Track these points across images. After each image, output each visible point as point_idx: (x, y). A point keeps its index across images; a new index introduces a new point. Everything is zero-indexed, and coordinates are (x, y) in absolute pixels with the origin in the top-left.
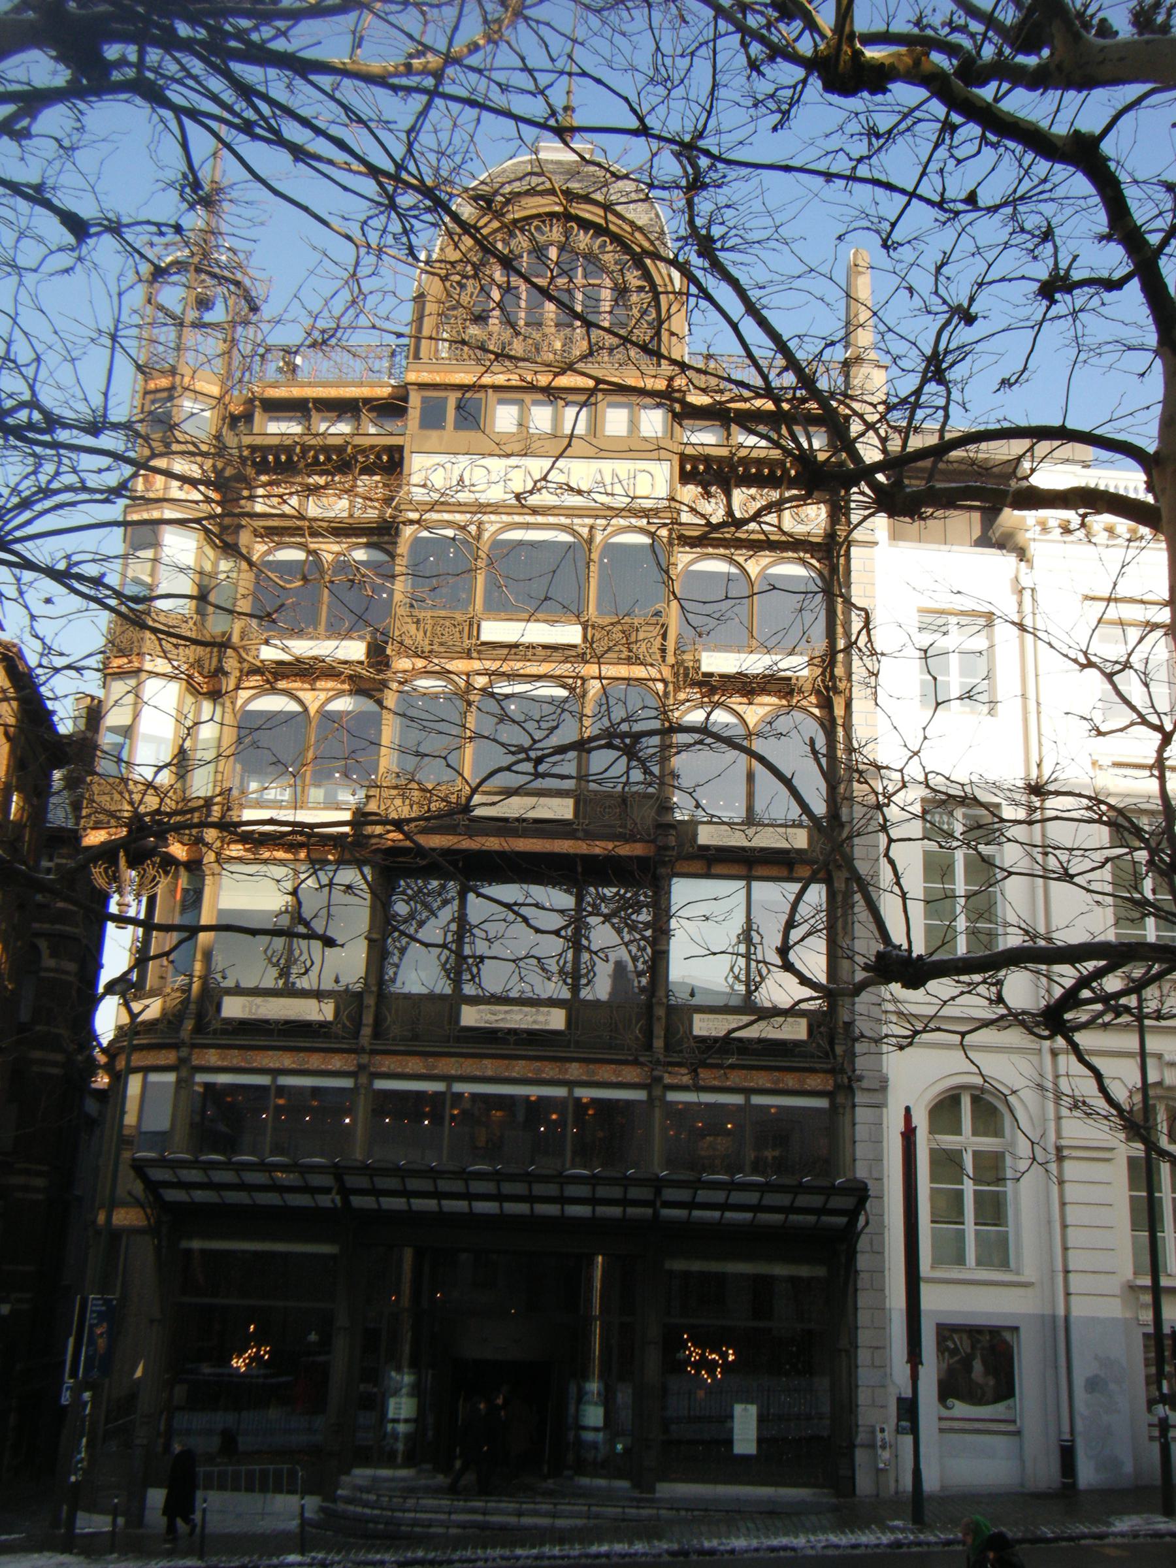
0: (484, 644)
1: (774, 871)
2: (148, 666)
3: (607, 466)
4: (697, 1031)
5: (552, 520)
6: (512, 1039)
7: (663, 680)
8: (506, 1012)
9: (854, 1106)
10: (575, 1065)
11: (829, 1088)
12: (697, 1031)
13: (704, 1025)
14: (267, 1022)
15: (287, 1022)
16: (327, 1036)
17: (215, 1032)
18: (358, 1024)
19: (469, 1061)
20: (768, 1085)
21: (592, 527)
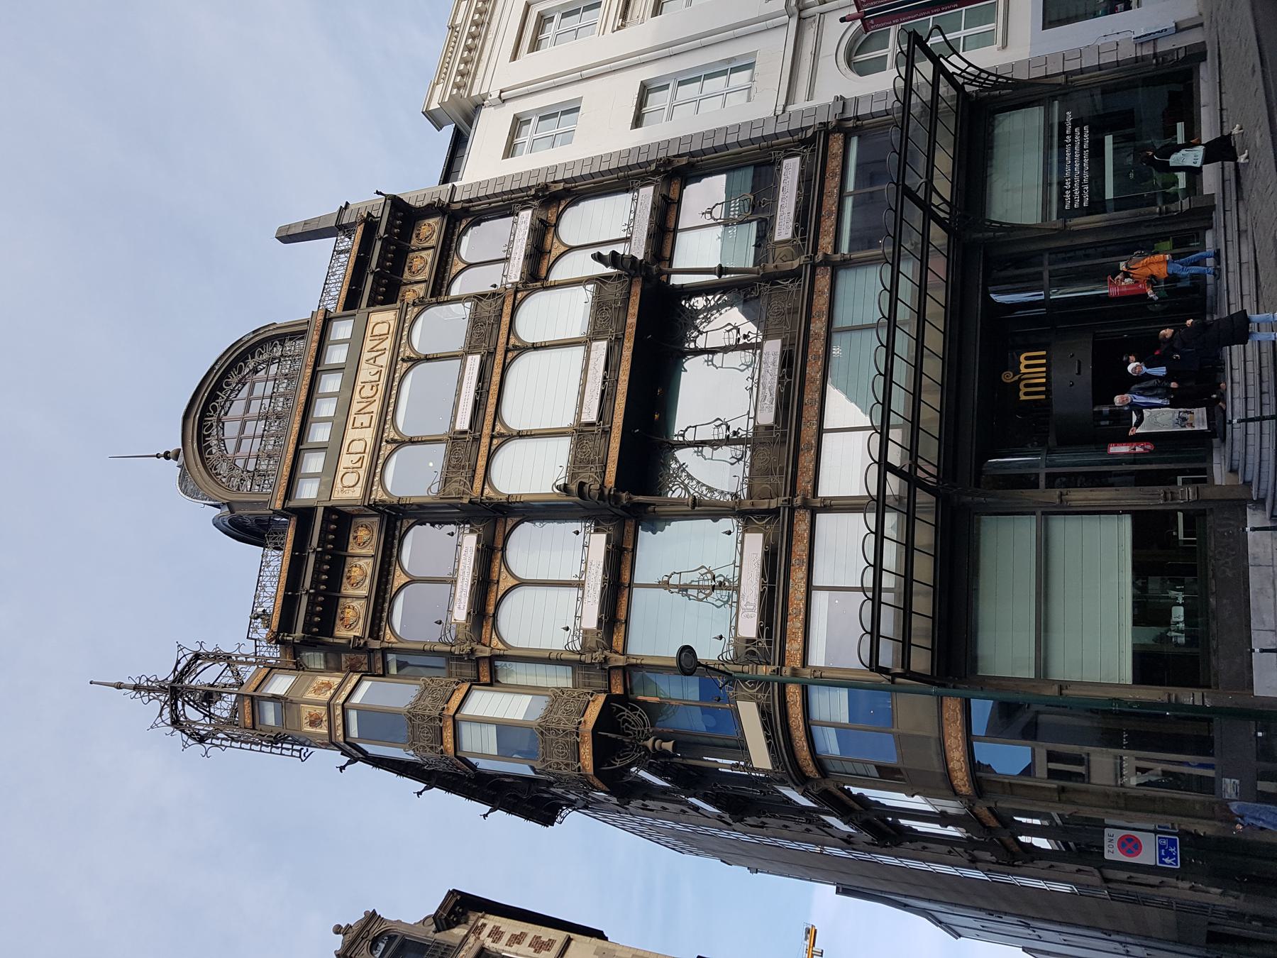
0: (470, 427)
1: (672, 215)
3: (366, 355)
7: (516, 292)
9: (857, 118)
11: (841, 136)
12: (789, 236)
14: (762, 593)
15: (763, 576)
17: (769, 643)
18: (768, 512)
19: (805, 414)
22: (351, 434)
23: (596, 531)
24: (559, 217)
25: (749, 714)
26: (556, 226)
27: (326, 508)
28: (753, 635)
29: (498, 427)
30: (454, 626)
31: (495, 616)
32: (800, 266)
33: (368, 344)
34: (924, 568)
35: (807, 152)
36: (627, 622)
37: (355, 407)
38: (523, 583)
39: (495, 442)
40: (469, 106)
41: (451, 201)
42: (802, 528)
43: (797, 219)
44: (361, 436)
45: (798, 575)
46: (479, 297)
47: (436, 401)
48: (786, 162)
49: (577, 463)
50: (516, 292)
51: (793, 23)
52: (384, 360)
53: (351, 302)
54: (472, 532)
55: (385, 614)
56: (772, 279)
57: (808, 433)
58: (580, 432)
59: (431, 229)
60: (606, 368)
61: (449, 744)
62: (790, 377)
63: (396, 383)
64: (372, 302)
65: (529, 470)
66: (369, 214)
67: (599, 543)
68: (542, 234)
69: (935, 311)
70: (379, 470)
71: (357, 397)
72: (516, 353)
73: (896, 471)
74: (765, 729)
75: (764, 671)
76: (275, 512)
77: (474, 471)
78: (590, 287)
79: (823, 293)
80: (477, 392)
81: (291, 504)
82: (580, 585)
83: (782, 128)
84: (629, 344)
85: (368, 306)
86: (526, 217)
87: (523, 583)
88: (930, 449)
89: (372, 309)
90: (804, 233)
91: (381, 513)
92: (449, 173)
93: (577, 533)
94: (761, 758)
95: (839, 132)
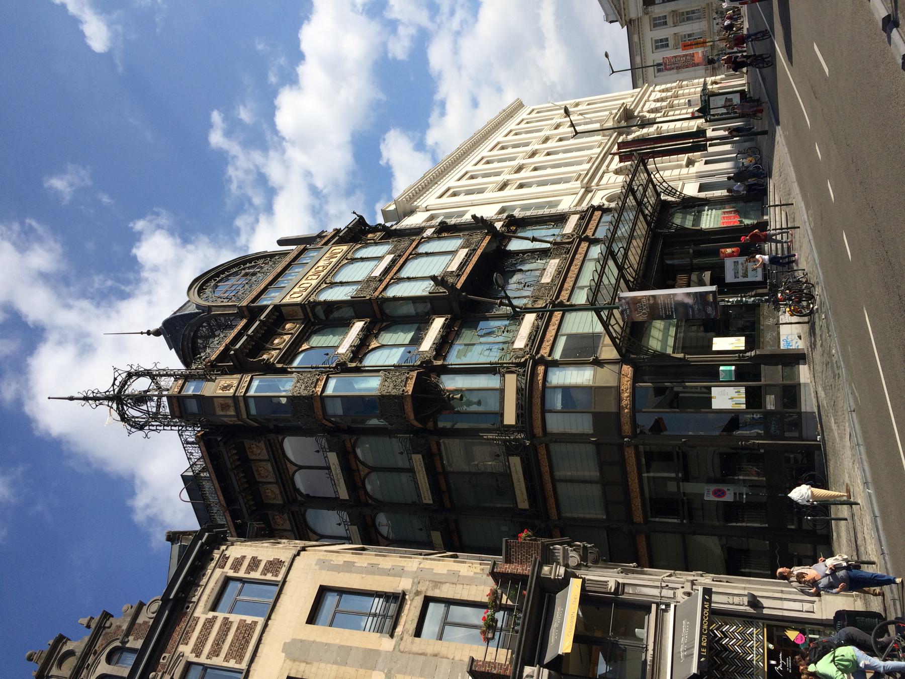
3: (324, 258)
33: (327, 255)
37: (310, 273)
40: (408, 207)
47: (358, 272)
51: (583, 190)
52: (334, 260)
57: (569, 284)
61: (319, 389)
71: (313, 270)
74: (517, 393)
75: (523, 360)
83: (573, 210)
84: (479, 252)
87: (382, 346)
94: (510, 418)
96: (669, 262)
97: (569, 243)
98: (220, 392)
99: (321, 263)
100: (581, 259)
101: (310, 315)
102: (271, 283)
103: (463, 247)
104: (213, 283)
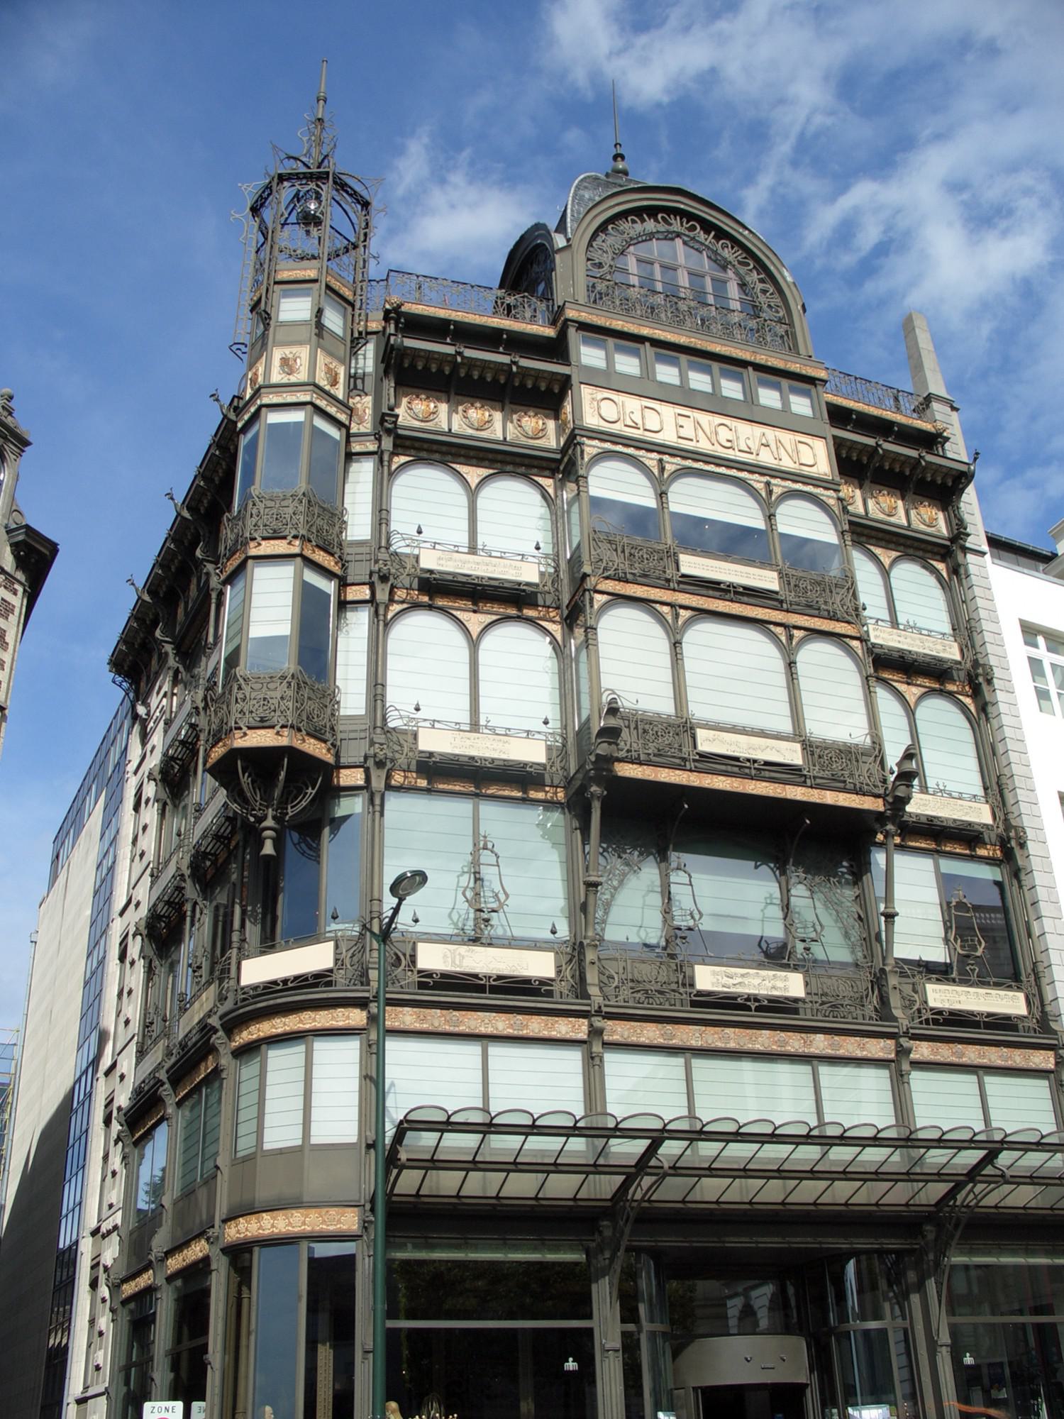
0: (683, 576)
2: (308, 553)
3: (771, 434)
4: (932, 1004)
5: (722, 470)
6: (753, 1005)
8: (743, 976)
10: (820, 1037)
12: (932, 1004)
13: (937, 996)
14: (476, 976)
15: (500, 978)
16: (549, 994)
19: (711, 1030)
20: (1000, 1063)
21: (768, 484)
22: (668, 411)
23: (549, 748)
24: (950, 695)
25: (313, 958)
26: (943, 693)
27: (568, 377)
28: (422, 963)
29: (685, 614)
30: (416, 552)
31: (430, 607)
32: (895, 1019)
33: (787, 438)
34: (521, 1186)
35: (1033, 1024)
36: (428, 791)
37: (704, 418)
38: (474, 644)
39: (666, 609)
41: (965, 550)
42: (563, 1028)
43: (952, 1013)
44: (667, 423)
45: (501, 1023)
46: (848, 584)
48: (1021, 996)
49: (644, 724)
50: (863, 639)
52: (766, 458)
53: (838, 416)
54: (542, 574)
55: (424, 454)
56: (879, 981)
58: (685, 727)
59: (929, 521)
60: (767, 763)
61: (268, 548)
62: (757, 1009)
63: (733, 472)
64: (839, 444)
65: (630, 657)
66: (947, 439)
67: (533, 753)
68: (934, 674)
69: (842, 1191)
70: (619, 448)
71: (718, 419)
72: (783, 639)
73: (652, 1150)
74: (296, 978)
76: (561, 309)
77: (627, 582)
78: (868, 740)
79: (863, 1049)
80: (730, 585)
81: (572, 332)
82: (475, 726)
85: (835, 437)
86: (951, 652)
87: (474, 644)
88: (672, 1190)
89: (832, 443)
90: (936, 1022)
91: (564, 451)
92: (999, 545)
93: (546, 722)
94: (258, 970)
95: (1057, 1064)
96: (851, 1267)
97: (883, 1011)
98: (278, 354)
99: (744, 429)
100: (813, 1050)
101: (566, 459)
102: (656, 343)
103: (809, 747)
104: (676, 225)
